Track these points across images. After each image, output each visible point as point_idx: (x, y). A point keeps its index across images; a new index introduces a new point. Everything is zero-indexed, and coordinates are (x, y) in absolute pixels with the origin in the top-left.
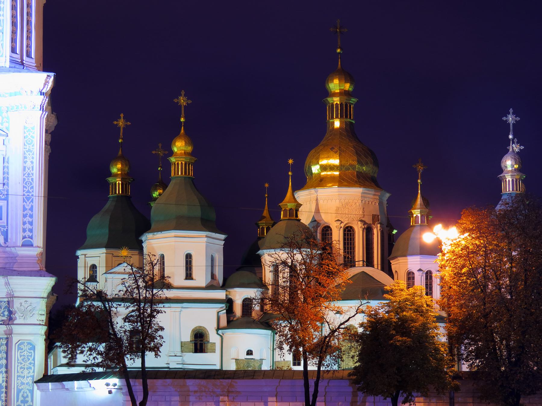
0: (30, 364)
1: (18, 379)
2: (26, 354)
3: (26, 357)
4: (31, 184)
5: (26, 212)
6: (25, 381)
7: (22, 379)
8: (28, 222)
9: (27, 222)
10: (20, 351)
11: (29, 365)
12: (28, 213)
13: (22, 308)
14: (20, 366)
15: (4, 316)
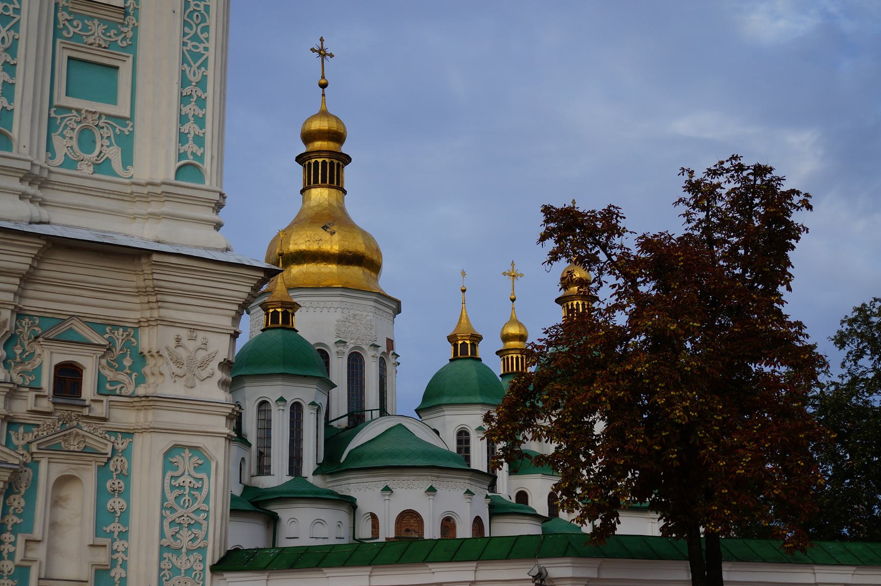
0: (198, 511)
1: (161, 558)
2: (187, 484)
3: (187, 492)
4: (204, 20)
5: (187, 91)
6: (182, 563)
7: (174, 560)
8: (194, 115)
9: (190, 116)
10: (169, 474)
11: (193, 516)
12: (194, 93)
13: (180, 351)
14: (174, 516)
15: (121, 369)
